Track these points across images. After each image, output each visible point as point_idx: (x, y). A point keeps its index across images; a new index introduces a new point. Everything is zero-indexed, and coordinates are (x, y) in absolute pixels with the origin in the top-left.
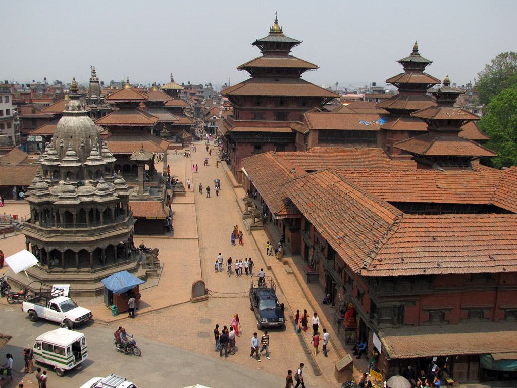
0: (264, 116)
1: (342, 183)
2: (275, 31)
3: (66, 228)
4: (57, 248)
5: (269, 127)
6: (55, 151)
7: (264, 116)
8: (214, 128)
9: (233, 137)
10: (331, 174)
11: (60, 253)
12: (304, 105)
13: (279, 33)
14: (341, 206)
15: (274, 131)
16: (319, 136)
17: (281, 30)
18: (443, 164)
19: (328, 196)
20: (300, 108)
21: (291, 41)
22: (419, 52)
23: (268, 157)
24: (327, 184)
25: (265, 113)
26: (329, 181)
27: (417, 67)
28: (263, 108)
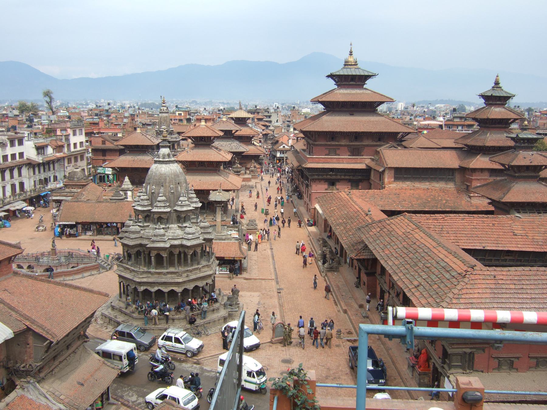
0: (338, 152)
1: (417, 230)
2: (350, 63)
3: (156, 269)
4: (149, 288)
5: (343, 163)
8: (283, 157)
9: (306, 173)
10: (406, 221)
11: (150, 292)
12: (379, 140)
13: (354, 65)
14: (417, 255)
16: (395, 174)
17: (356, 62)
18: (521, 211)
19: (404, 243)
20: (375, 143)
21: (366, 74)
22: (500, 85)
23: (343, 196)
24: (403, 231)
25: (339, 149)
26: (405, 228)
27: (498, 101)
28: (337, 143)
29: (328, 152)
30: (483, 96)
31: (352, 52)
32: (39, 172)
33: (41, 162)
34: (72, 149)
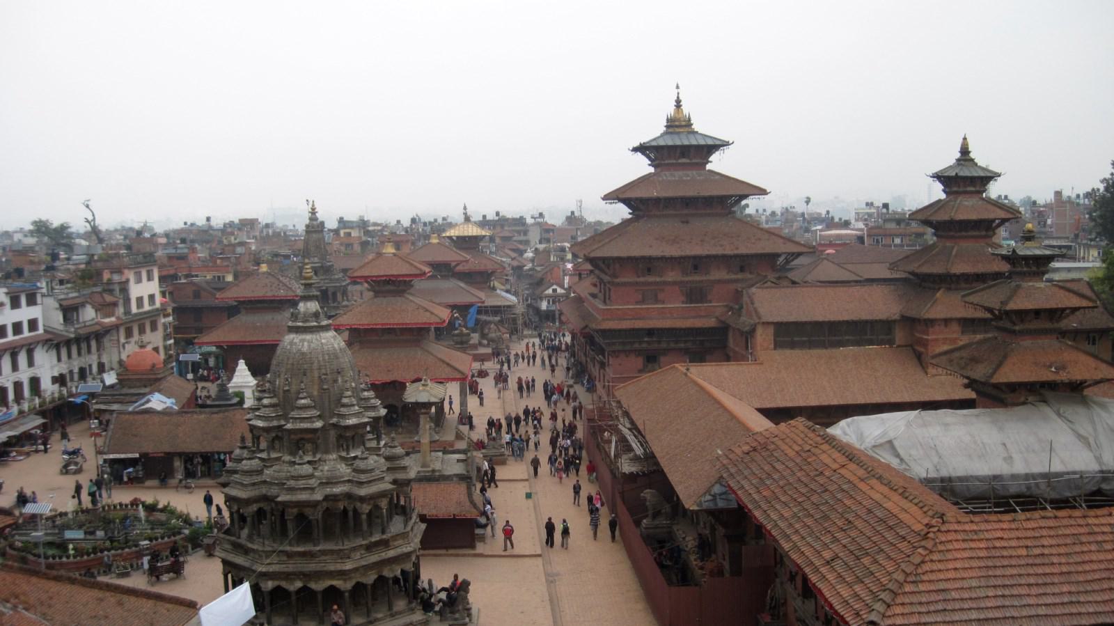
1: (825, 447)
2: (677, 123)
6: (274, 401)
7: (661, 296)
8: (554, 311)
9: (599, 339)
12: (742, 269)
13: (686, 126)
14: (826, 496)
15: (683, 326)
16: (776, 335)
19: (799, 474)
20: (733, 277)
21: (710, 142)
22: (972, 155)
26: (800, 442)
28: (658, 279)
29: (640, 297)
30: (939, 177)
31: (680, 101)
32: (69, 356)
33: (72, 336)
34: (134, 309)
